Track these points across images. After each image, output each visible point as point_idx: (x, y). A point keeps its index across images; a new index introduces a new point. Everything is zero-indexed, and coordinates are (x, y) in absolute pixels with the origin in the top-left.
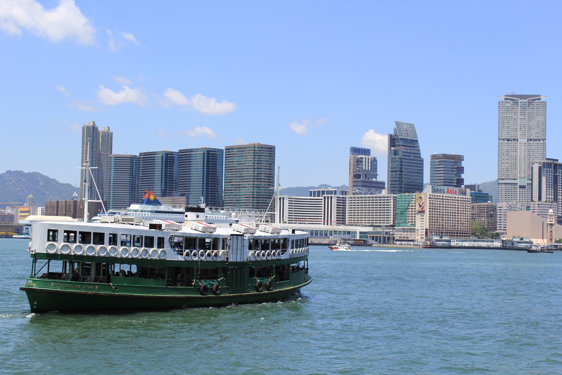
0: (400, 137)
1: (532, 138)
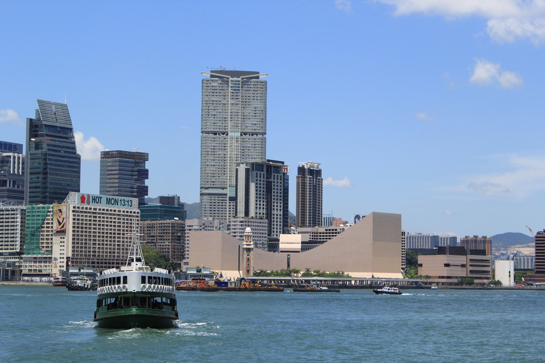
0: (44, 123)
1: (246, 131)
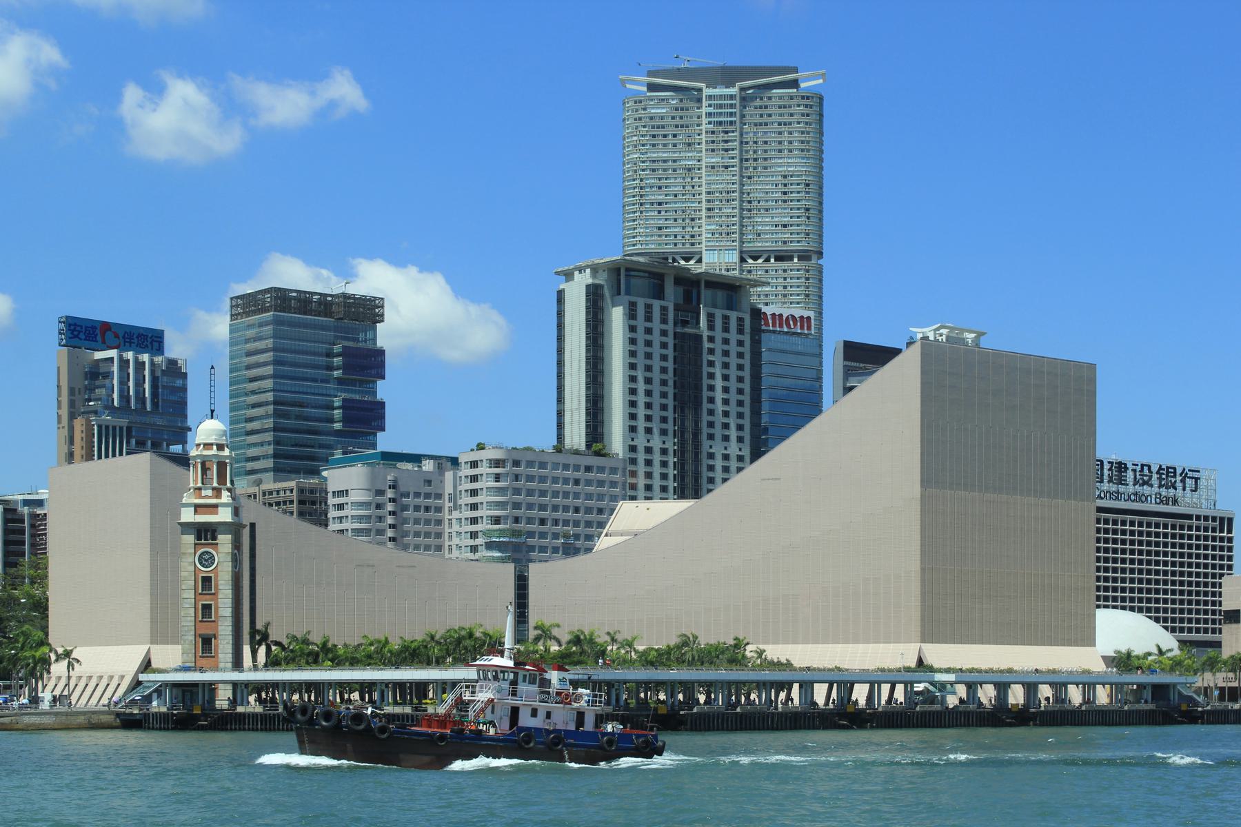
1: (759, 245)
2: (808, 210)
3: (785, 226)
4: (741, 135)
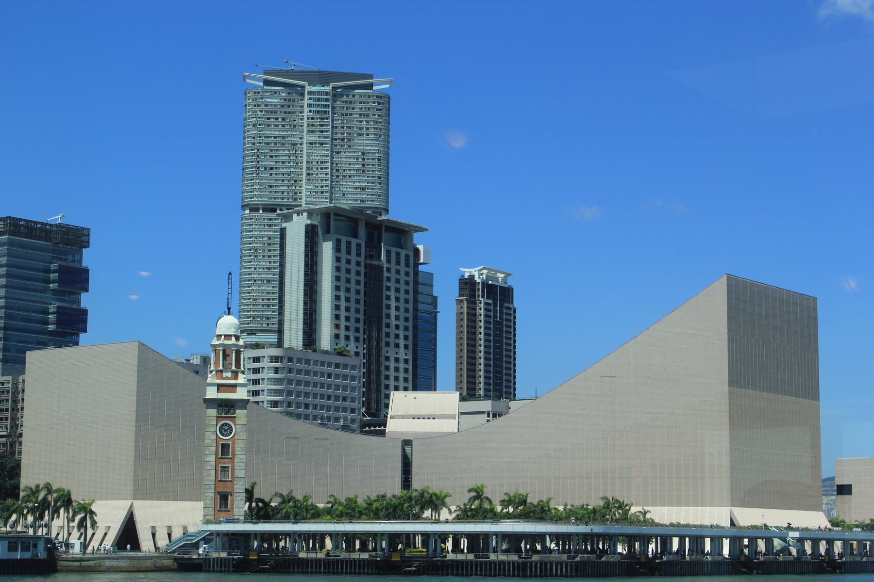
2: (379, 178)
3: (363, 189)
4: (332, 121)
